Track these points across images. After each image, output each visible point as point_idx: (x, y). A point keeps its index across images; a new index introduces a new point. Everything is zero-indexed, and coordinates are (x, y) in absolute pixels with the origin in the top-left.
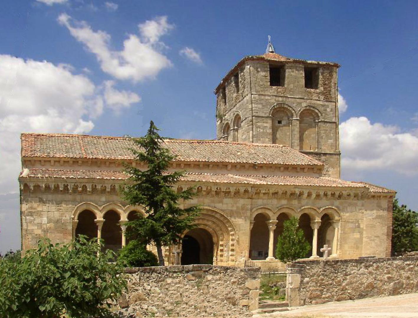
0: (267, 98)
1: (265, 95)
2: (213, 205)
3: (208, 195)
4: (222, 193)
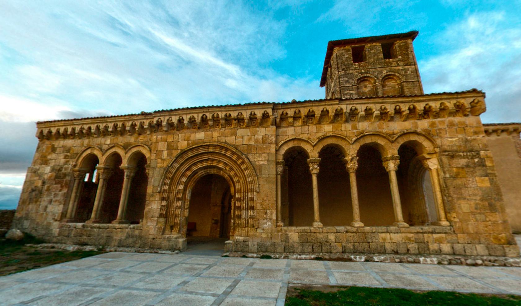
0: (351, 71)
4: (233, 121)
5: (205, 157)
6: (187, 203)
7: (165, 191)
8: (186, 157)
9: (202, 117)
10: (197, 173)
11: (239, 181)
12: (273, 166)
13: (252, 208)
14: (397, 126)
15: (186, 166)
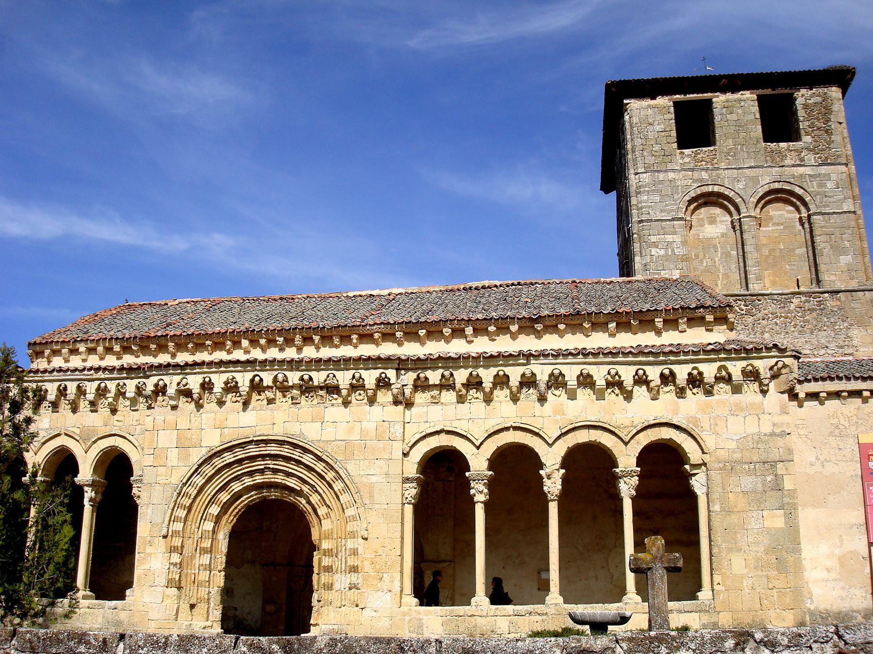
0: (671, 175)
1: (666, 171)
3: (284, 400)
5: (259, 464)
6: (221, 560)
7: (175, 533)
8: (218, 462)
9: (252, 380)
10: (241, 496)
11: (328, 516)
12: (397, 486)
13: (354, 569)
14: (644, 408)
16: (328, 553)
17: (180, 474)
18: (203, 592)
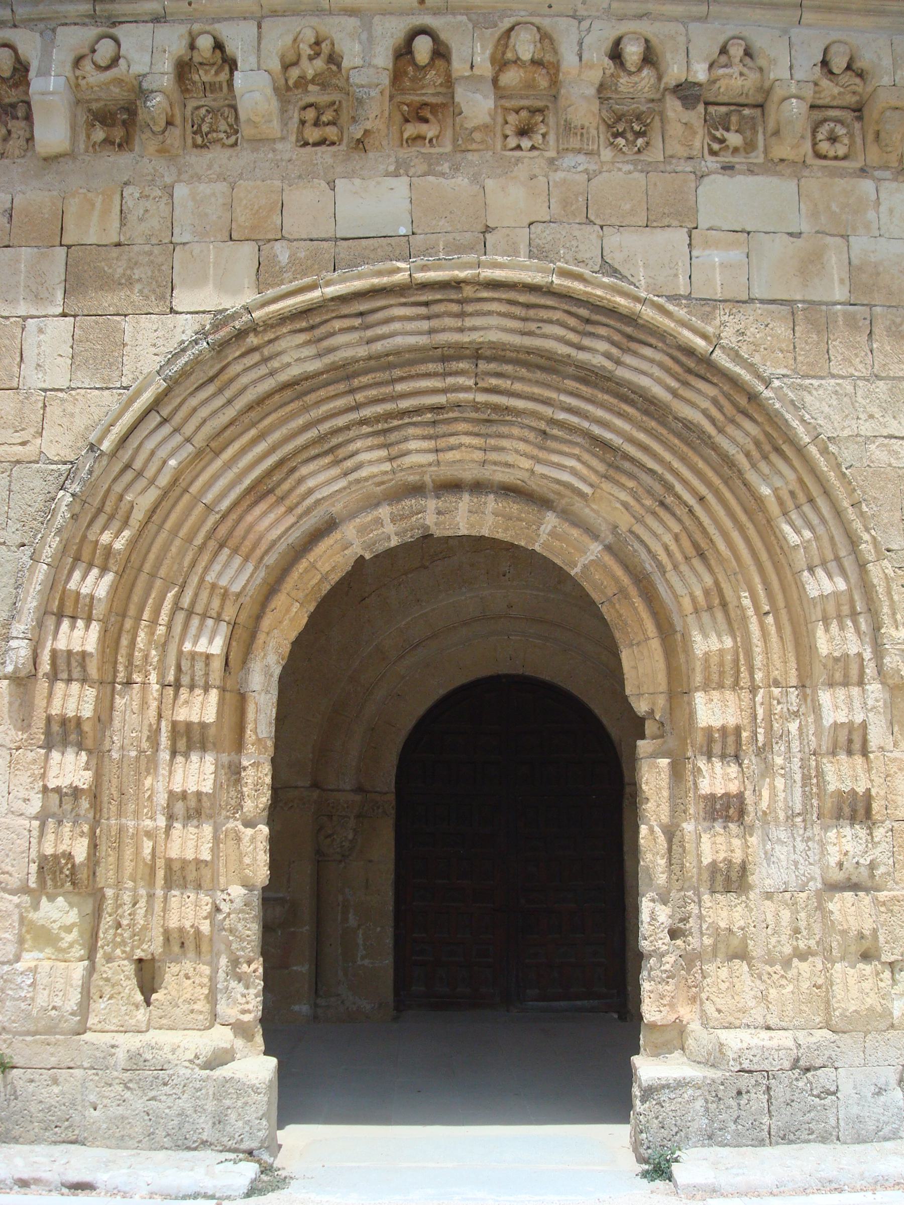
2: (587, 243)
3: (526, 143)
5: (425, 388)
7: (68, 666)
13: (857, 810)
15: (249, 460)
16: (727, 745)
17: (80, 423)
18: (187, 911)
